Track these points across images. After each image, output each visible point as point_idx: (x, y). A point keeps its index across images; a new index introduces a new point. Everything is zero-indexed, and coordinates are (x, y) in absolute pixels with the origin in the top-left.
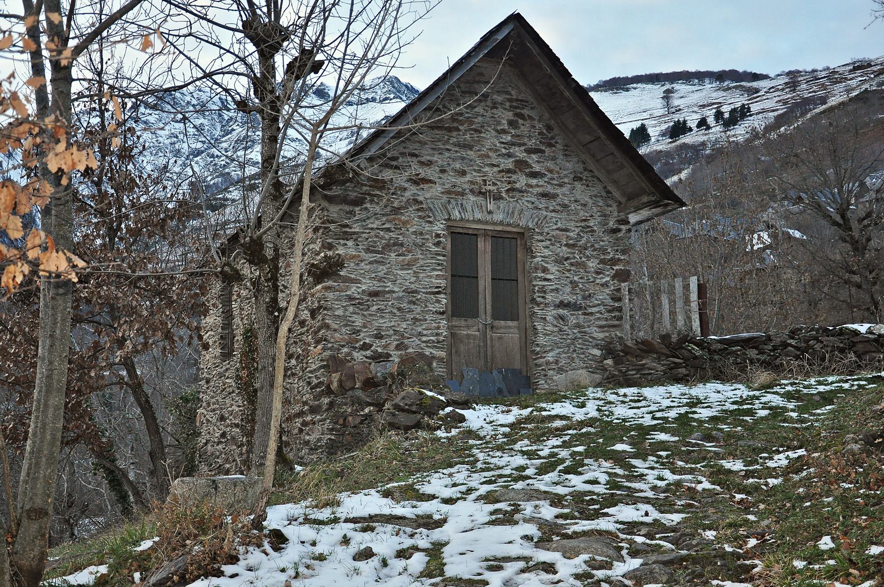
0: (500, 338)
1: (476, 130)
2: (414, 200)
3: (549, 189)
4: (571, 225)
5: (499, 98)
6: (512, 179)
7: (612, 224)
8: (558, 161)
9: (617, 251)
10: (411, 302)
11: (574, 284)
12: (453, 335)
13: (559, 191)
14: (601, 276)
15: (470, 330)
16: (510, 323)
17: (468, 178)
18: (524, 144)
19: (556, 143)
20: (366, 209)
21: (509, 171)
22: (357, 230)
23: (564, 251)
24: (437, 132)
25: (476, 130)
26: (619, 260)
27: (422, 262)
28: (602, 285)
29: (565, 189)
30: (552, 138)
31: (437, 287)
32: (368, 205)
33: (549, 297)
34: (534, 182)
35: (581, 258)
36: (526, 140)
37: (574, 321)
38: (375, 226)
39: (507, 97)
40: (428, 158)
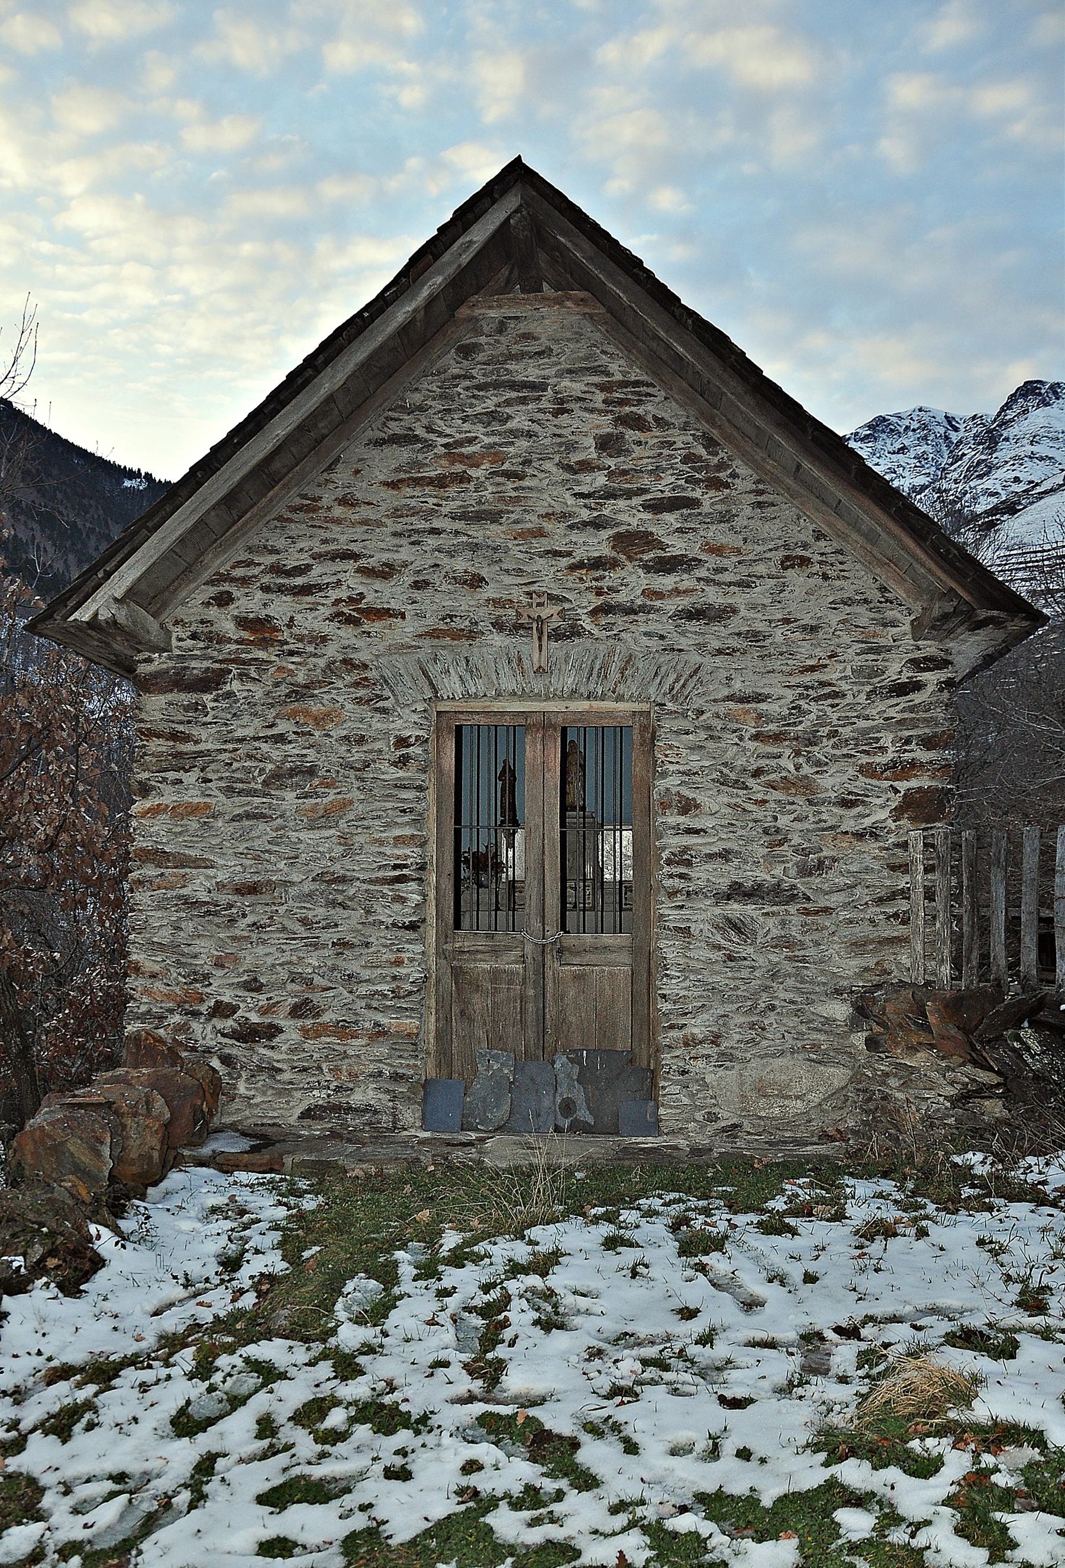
0: (579, 977)
1: (509, 475)
2: (344, 661)
3: (713, 596)
4: (772, 685)
5: (573, 387)
6: (605, 584)
7: (896, 670)
8: (739, 522)
9: (908, 741)
10: (334, 904)
11: (776, 838)
12: (457, 973)
13: (739, 599)
14: (859, 809)
15: (499, 959)
16: (607, 939)
17: (490, 592)
18: (643, 491)
19: (734, 475)
20: (230, 695)
21: (598, 563)
22: (210, 746)
23: (747, 754)
24: (408, 491)
25: (509, 475)
26: (913, 764)
27: (360, 809)
28: (860, 836)
29: (759, 593)
30: (721, 466)
31: (396, 867)
32: (235, 686)
33: (702, 874)
34: (667, 582)
35: (798, 767)
36: (646, 481)
37: (775, 932)
38: (249, 732)
39: (596, 379)
40: (385, 557)
